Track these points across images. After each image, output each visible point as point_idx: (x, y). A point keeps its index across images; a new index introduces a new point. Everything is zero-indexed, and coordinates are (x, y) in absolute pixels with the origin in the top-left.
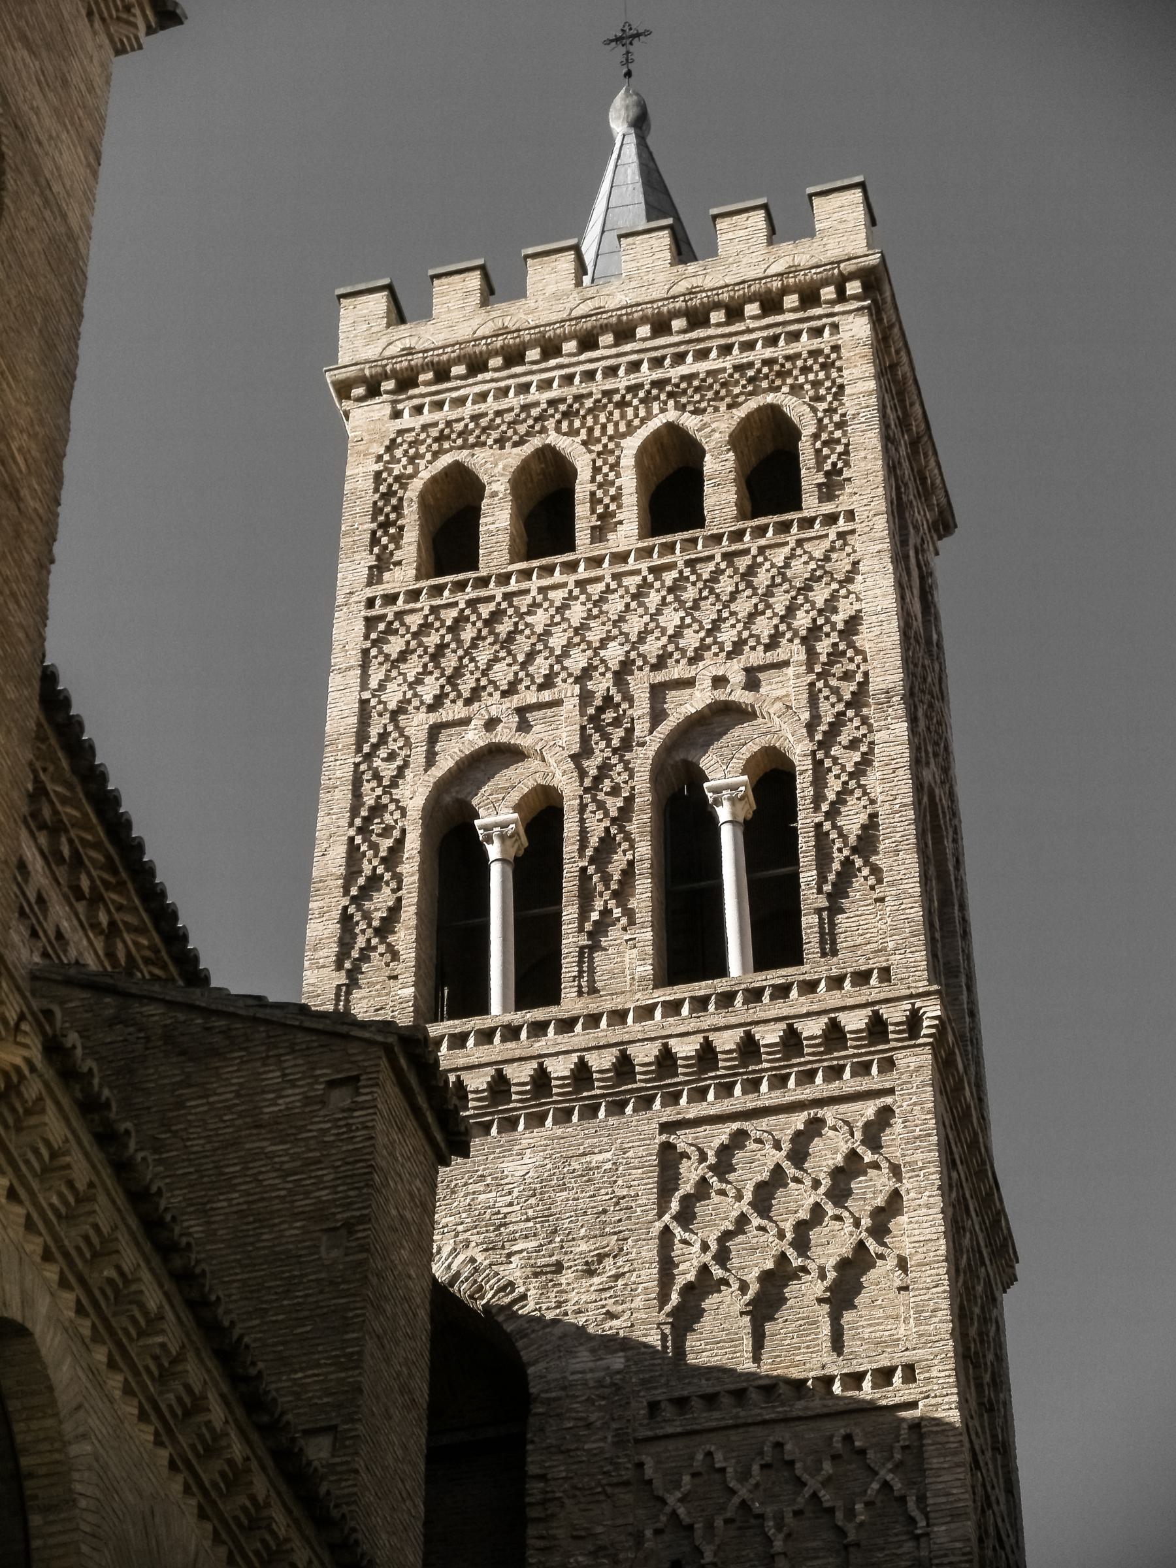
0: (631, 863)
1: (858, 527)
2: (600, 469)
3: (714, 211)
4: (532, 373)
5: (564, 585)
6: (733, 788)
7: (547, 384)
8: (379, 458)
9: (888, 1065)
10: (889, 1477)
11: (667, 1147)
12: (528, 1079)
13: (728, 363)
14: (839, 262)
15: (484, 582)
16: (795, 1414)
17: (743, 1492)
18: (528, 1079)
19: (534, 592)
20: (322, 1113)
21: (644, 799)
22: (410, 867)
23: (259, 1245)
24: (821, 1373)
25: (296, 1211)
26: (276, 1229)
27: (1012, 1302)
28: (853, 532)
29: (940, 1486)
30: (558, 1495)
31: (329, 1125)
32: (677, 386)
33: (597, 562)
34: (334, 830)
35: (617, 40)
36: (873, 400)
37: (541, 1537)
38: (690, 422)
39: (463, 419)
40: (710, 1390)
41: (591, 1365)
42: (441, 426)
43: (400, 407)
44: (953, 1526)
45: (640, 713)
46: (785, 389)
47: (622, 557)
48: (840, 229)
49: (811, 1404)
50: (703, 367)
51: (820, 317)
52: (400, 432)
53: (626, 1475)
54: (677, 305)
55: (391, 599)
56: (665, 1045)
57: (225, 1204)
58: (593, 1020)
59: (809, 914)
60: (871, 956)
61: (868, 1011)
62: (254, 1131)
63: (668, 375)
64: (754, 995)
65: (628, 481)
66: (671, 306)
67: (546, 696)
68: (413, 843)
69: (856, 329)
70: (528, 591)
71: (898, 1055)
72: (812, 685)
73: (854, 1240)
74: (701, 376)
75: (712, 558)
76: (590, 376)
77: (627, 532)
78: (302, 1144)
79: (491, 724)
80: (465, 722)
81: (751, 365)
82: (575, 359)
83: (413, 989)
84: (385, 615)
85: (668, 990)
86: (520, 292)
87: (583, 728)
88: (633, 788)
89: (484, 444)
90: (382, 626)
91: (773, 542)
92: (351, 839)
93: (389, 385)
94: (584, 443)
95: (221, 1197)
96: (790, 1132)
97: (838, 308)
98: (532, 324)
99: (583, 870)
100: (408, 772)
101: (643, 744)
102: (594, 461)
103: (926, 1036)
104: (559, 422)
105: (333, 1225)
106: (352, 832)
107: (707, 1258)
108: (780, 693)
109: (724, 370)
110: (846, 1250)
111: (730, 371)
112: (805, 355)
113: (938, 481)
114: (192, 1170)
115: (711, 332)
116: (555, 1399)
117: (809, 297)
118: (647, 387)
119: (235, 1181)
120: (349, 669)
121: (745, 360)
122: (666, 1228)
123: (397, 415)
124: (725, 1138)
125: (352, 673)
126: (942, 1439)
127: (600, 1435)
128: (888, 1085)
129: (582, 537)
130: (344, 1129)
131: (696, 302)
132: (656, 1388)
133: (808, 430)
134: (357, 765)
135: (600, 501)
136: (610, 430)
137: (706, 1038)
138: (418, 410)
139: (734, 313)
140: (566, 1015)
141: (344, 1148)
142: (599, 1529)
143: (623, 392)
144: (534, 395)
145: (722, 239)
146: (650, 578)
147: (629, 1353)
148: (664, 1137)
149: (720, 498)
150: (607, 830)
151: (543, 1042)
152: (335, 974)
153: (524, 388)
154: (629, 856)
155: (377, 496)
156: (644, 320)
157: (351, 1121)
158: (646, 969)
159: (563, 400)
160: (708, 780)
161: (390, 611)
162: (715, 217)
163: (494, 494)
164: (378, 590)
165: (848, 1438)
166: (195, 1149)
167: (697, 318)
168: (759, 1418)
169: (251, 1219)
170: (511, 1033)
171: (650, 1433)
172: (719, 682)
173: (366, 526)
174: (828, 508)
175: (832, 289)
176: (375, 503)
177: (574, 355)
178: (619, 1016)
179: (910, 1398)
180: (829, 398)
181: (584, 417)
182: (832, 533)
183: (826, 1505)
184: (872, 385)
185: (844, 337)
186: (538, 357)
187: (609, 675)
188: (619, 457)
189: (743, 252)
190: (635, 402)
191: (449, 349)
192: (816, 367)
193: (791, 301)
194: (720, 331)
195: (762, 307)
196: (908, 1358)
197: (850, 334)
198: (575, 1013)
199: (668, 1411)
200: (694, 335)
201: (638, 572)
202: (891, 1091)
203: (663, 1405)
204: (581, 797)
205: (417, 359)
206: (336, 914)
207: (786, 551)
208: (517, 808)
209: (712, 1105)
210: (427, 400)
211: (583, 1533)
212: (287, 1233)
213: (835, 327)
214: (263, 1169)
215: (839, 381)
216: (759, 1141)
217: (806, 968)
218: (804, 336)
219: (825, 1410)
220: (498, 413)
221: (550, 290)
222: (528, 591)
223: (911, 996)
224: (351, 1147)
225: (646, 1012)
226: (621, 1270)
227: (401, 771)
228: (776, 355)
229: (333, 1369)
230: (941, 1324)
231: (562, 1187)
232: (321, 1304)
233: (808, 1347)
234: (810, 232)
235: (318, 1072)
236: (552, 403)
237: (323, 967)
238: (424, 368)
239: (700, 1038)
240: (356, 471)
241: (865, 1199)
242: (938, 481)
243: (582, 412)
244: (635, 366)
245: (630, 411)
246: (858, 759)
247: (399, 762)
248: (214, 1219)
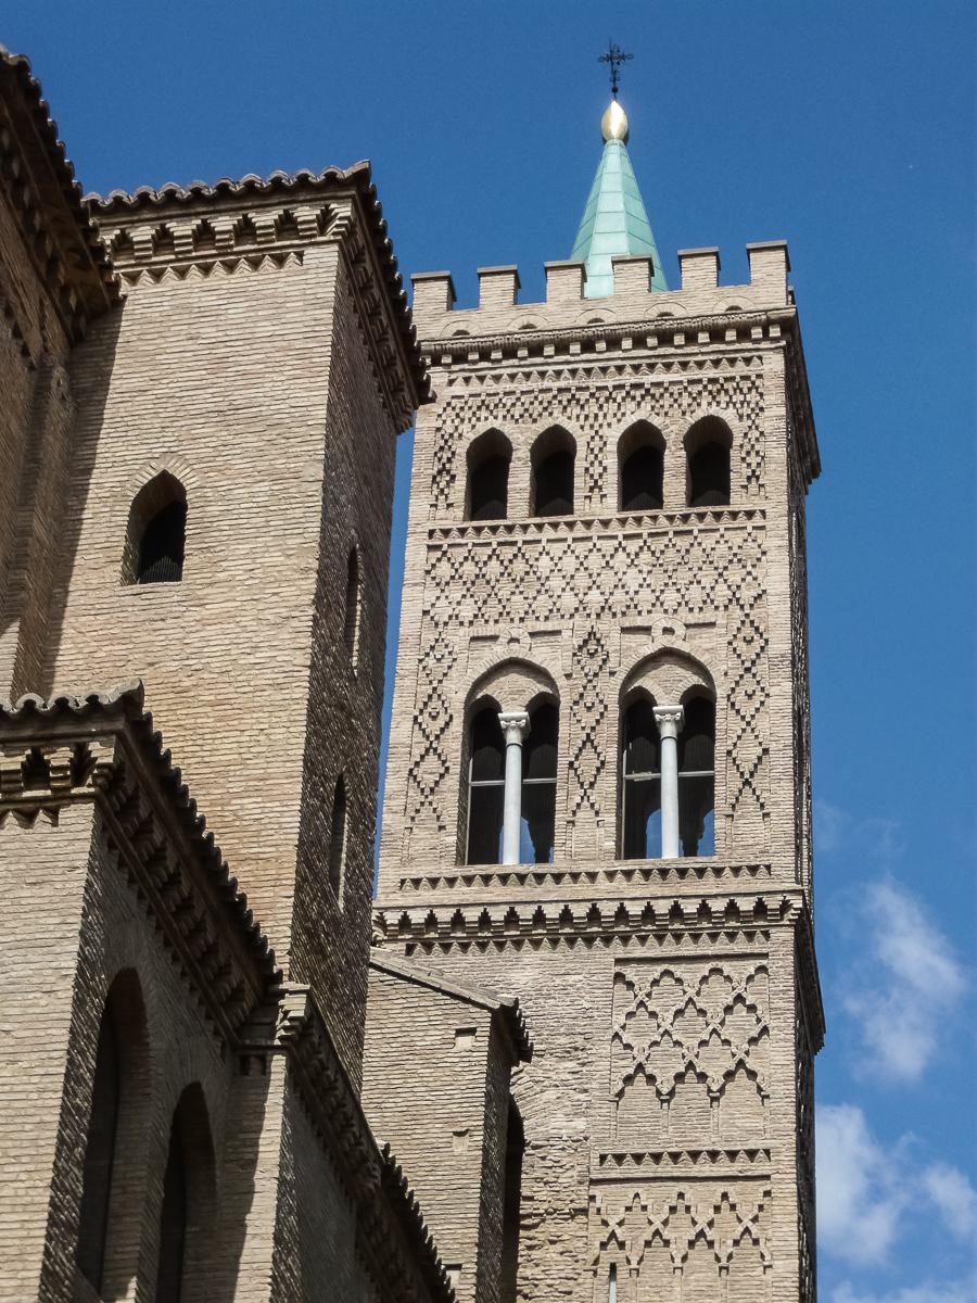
0: (603, 763)
1: (767, 523)
2: (592, 450)
3: (681, 252)
4: (548, 364)
5: (565, 540)
6: (673, 713)
7: (558, 373)
8: (440, 416)
9: (767, 935)
10: (750, 1224)
11: (619, 977)
12: (531, 917)
13: (684, 376)
14: (766, 311)
15: (510, 529)
16: (691, 1175)
17: (658, 1224)
18: (531, 917)
19: (544, 543)
20: (454, 1050)
21: (614, 713)
22: (454, 743)
23: (414, 1136)
24: (710, 1148)
25: (438, 1116)
26: (425, 1127)
27: (818, 1059)
28: (763, 528)
29: (782, 1234)
30: (542, 1211)
31: (457, 1060)
32: (648, 391)
33: (588, 524)
34: (404, 709)
35: (610, 58)
36: (783, 424)
37: (530, 1239)
38: (656, 421)
39: (498, 394)
40: (639, 1151)
41: (565, 1124)
42: (483, 398)
43: (453, 376)
44: (787, 1262)
45: (613, 648)
46: (724, 405)
47: (605, 523)
48: (768, 285)
49: (703, 1169)
50: (665, 378)
51: (749, 350)
52: (453, 397)
53: (584, 1204)
54: (653, 327)
55: (446, 533)
56: (622, 904)
57: (393, 1105)
58: (575, 876)
59: (720, 818)
60: (758, 855)
61: (755, 899)
62: (411, 1057)
63: (642, 381)
64: (682, 873)
65: (612, 461)
66: (648, 327)
67: (549, 626)
68: (458, 727)
69: (775, 364)
70: (539, 541)
71: (772, 930)
72: (730, 643)
73: (737, 1058)
74: (666, 385)
75: (666, 533)
76: (588, 371)
77: (609, 506)
78: (440, 1070)
79: (513, 640)
80: (494, 638)
81: (699, 381)
82: (577, 358)
83: (455, 838)
84: (441, 546)
85: (623, 862)
86: (541, 297)
87: (575, 655)
88: (606, 707)
89: (513, 416)
90: (439, 554)
91: (708, 527)
92: (416, 718)
93: (447, 360)
94: (582, 427)
95: (391, 1100)
96: (699, 976)
97: (764, 345)
98: (551, 328)
99: (571, 764)
100: (453, 673)
101: (612, 674)
102: (588, 443)
103: (790, 920)
104: (565, 408)
105: (459, 1130)
106: (417, 713)
107: (641, 1059)
108: (708, 646)
109: (681, 382)
110: (731, 1065)
111: (686, 384)
112: (738, 379)
113: (814, 446)
114: (372, 1078)
115: (672, 350)
116: (541, 1147)
117: (744, 333)
118: (628, 388)
119: (399, 1090)
120: (416, 585)
121: (696, 377)
122: (616, 1035)
123: (451, 382)
124: (656, 975)
125: (418, 588)
126: (785, 1203)
127: (569, 1173)
128: (764, 951)
129: (578, 503)
130: (467, 1064)
131: (667, 325)
132: (605, 1145)
133: (737, 442)
134: (421, 661)
135: (592, 476)
136: (601, 418)
137: (648, 903)
138: (467, 380)
139: (691, 337)
140: (556, 871)
141: (467, 1078)
142: (565, 1237)
143: (611, 390)
144: (547, 384)
145: (685, 275)
146: (624, 543)
147: (589, 1119)
148: (618, 969)
149: (674, 485)
150: (588, 735)
151: (539, 889)
152: (403, 819)
153: (542, 374)
154: (602, 758)
155: (437, 449)
156: (627, 335)
157: (471, 1059)
158: (610, 845)
159: (568, 390)
160: (657, 705)
161: (445, 543)
162: (681, 257)
163: (519, 459)
164: (438, 525)
165: (725, 1196)
166: (374, 1064)
167: (665, 338)
168: (669, 1175)
169: (409, 1118)
170: (522, 878)
171: (601, 1176)
172: (668, 631)
173: (430, 471)
174: (749, 507)
175: (760, 330)
176: (436, 453)
177: (578, 355)
178: (592, 876)
179: (765, 1173)
180: (753, 416)
181: (582, 407)
182: (749, 525)
183: (708, 1238)
184: (782, 411)
185: (766, 368)
186: (553, 353)
187: (593, 616)
188: (605, 443)
189: (700, 293)
190: (619, 400)
191: (492, 339)
192: (745, 391)
193: (731, 335)
194: (679, 351)
195: (710, 337)
196: (768, 1144)
197: (771, 366)
198: (563, 870)
199: (610, 1162)
200: (661, 351)
201: (615, 537)
202: (765, 956)
203: (609, 1157)
204: (571, 708)
205: (467, 342)
206: (405, 773)
207: (717, 535)
208: (528, 708)
209: (652, 949)
210: (473, 374)
211: (555, 1238)
212: (432, 1131)
213: (760, 358)
214: (416, 1084)
215: (761, 404)
216: (679, 981)
217: (715, 858)
218: (740, 365)
219: (713, 1174)
220: (523, 393)
221: (563, 298)
222: (539, 541)
223: (784, 892)
224: (471, 1077)
225: (611, 875)
226: (586, 1060)
227: (450, 667)
228: (717, 376)
229: (459, 1226)
230: (789, 1124)
231: (549, 997)
232: (453, 1182)
233: (703, 1128)
234: (747, 280)
235: (450, 1022)
236: (560, 390)
237: (396, 812)
238: (472, 350)
239: (645, 903)
240: (422, 425)
241: (744, 1029)
242: (814, 446)
243: (581, 403)
244: (620, 369)
245: (613, 407)
246: (758, 706)
247: (446, 662)
248: (386, 1114)
